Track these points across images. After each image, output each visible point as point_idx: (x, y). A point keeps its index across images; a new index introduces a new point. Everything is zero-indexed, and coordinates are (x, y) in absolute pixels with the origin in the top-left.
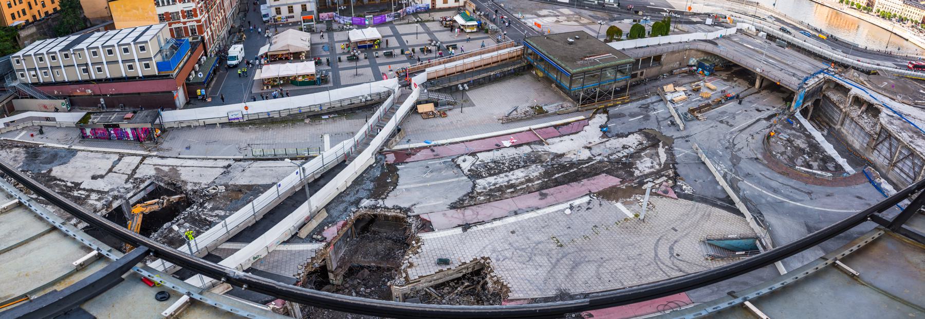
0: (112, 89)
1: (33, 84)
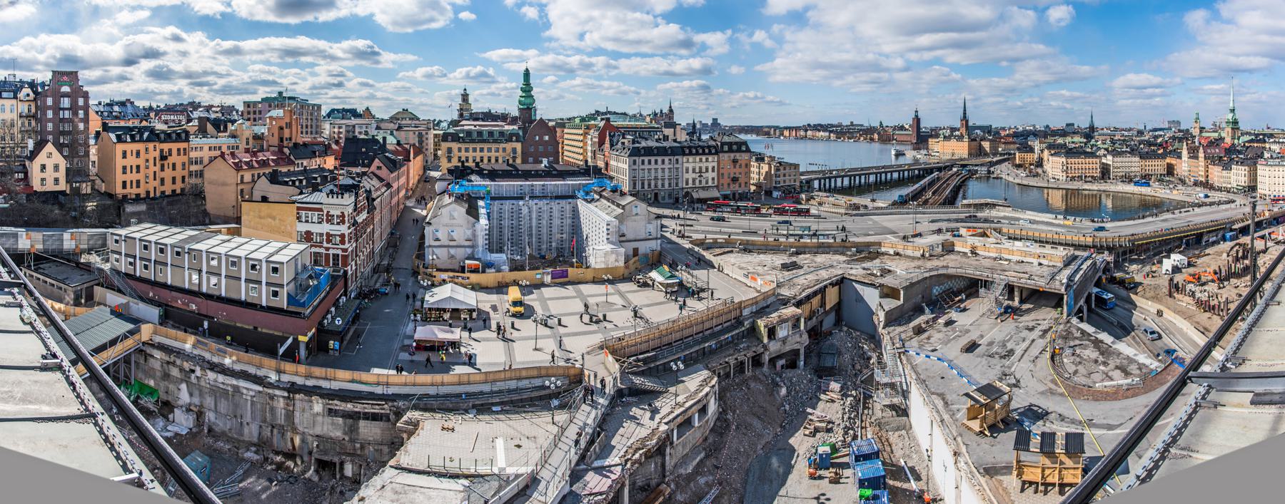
0: (223, 314)
1: (126, 274)
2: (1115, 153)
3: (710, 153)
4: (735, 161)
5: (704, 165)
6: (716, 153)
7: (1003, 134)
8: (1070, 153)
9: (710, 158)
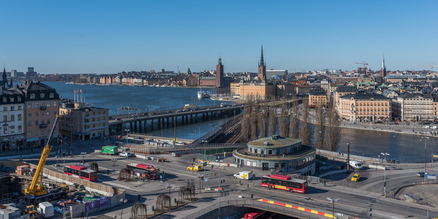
2: (406, 96)
3: (16, 102)
4: (43, 109)
5: (9, 114)
6: (23, 101)
7: (297, 78)
8: (361, 95)
9: (16, 106)
